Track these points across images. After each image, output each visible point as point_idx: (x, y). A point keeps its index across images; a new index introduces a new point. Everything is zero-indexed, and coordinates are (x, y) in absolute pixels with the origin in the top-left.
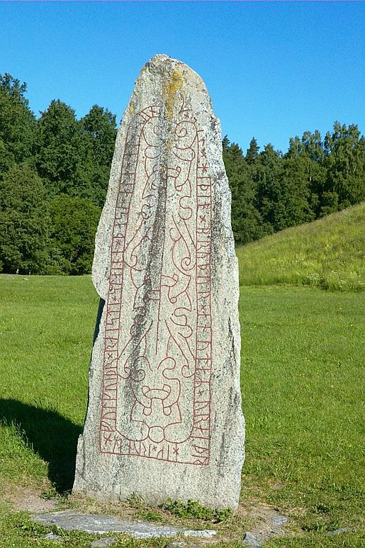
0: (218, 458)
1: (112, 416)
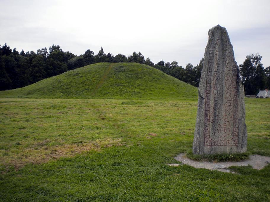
0: (241, 143)
1: (209, 134)
